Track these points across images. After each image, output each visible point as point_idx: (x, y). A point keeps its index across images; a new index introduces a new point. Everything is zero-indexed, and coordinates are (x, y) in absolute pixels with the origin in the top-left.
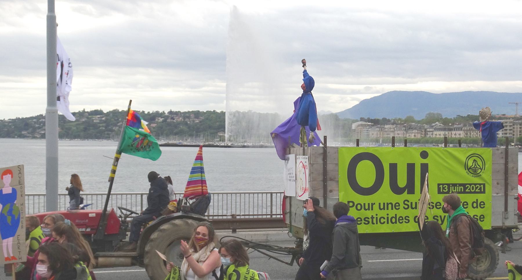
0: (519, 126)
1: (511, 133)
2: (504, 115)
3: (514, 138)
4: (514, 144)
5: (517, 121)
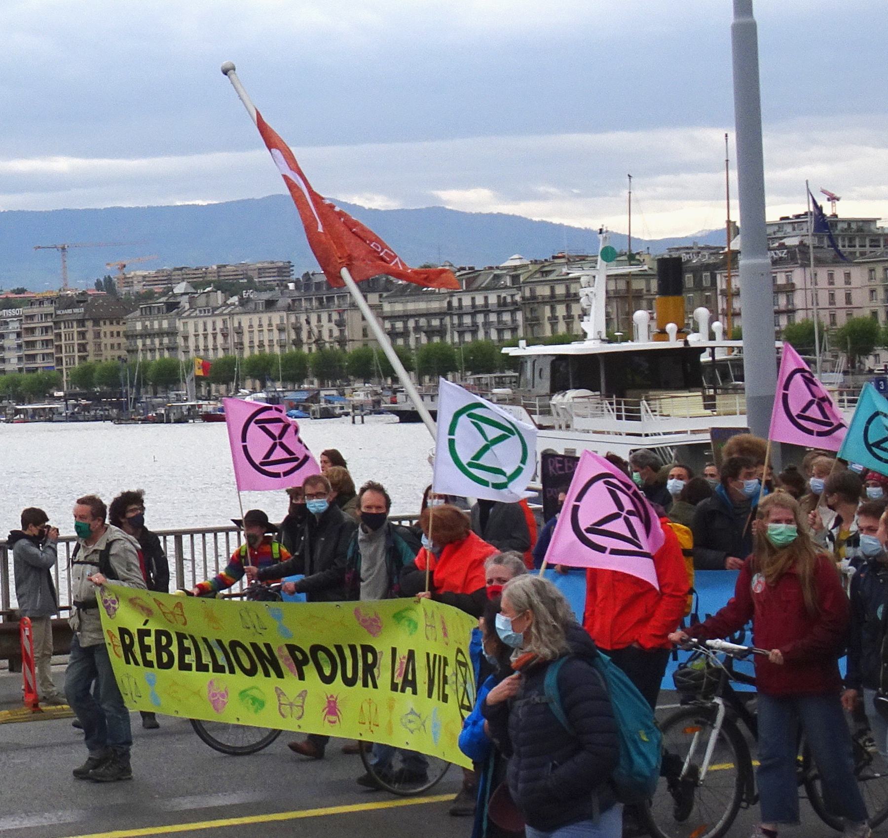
0: (76, 329)
1: (48, 354)
2: (21, 291)
3: (61, 371)
4: (61, 394)
5: (69, 311)
